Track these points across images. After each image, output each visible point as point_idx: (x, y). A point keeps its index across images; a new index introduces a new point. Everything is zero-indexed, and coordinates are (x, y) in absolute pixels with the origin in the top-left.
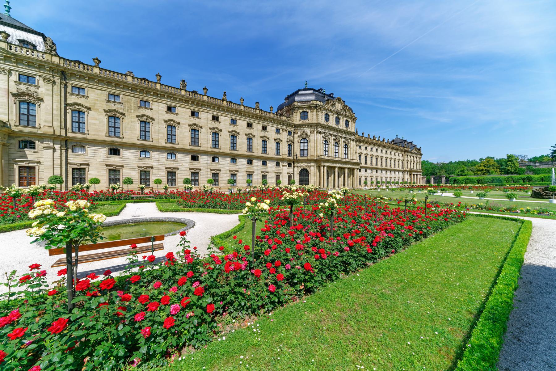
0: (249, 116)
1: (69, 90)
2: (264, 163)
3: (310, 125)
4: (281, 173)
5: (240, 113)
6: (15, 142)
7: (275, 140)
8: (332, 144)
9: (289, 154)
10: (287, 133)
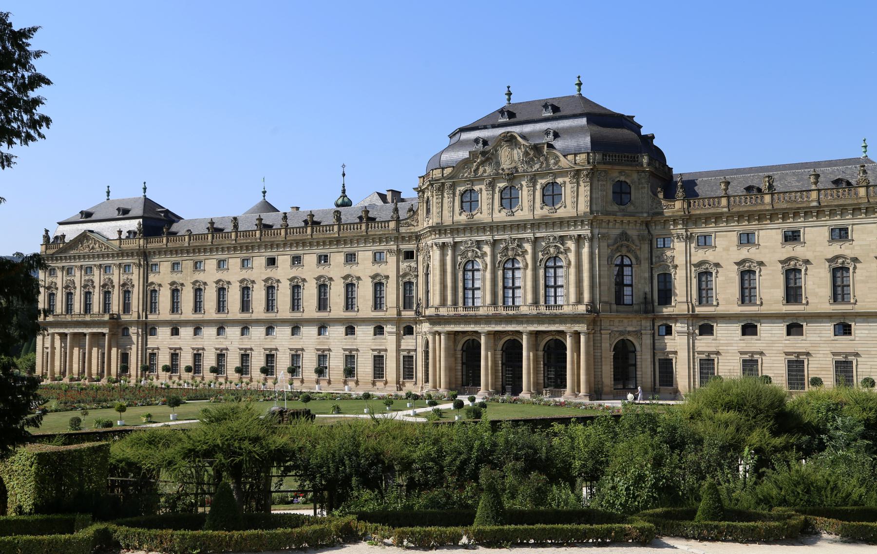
0: (318, 244)
1: (149, 269)
2: (350, 331)
4: (386, 350)
5: (303, 243)
6: (120, 330)
9: (407, 303)
10: (401, 257)
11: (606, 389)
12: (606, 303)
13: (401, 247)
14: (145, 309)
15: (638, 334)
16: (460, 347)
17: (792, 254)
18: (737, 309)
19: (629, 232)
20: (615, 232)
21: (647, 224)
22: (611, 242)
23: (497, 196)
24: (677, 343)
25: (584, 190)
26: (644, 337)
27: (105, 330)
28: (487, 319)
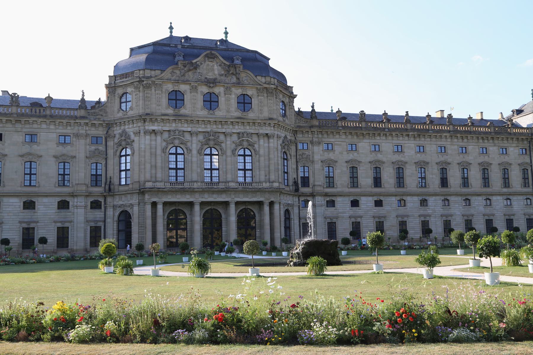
3: (132, 120)
4: (70, 222)
7: (55, 157)
8: (195, 152)
9: (96, 179)
10: (89, 140)
13: (89, 132)
16: (166, 217)
17: (376, 158)
18: (347, 190)
20: (283, 135)
21: (295, 132)
22: (280, 142)
23: (200, 98)
26: (295, 208)
28: (203, 191)
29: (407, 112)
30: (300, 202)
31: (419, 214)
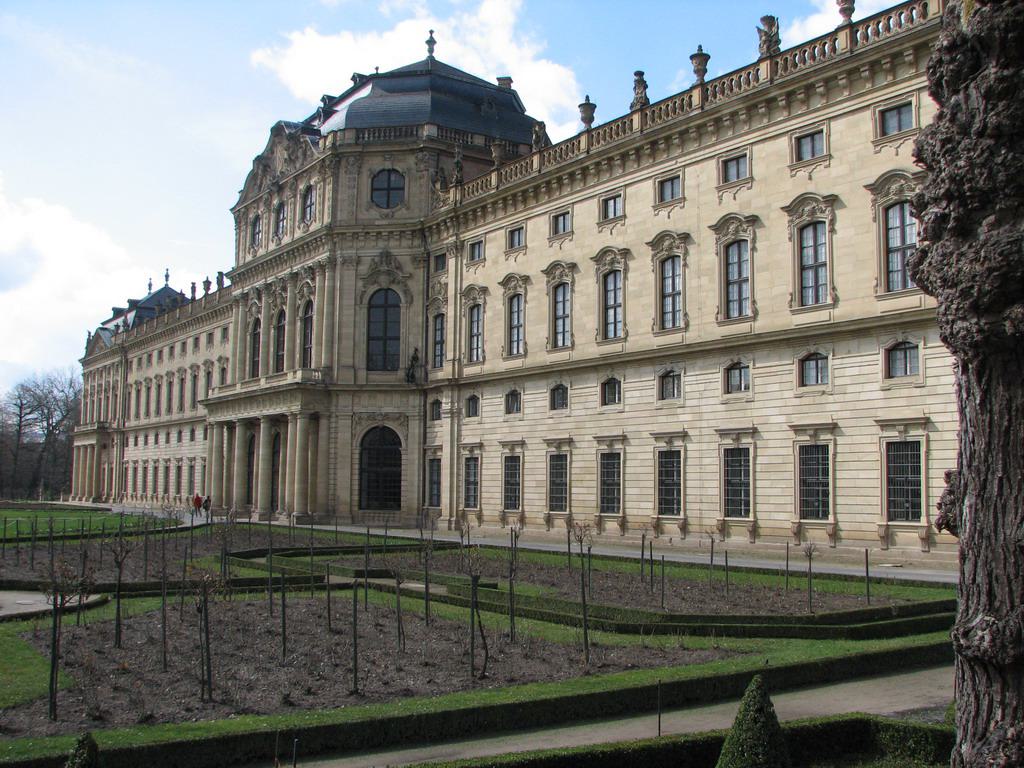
11: (344, 509)
12: (348, 367)
14: (124, 416)
15: (403, 419)
19: (394, 252)
20: (370, 251)
22: (364, 269)
24: (442, 430)
25: (329, 188)
27: (94, 442)
29: (640, 74)
30: (428, 406)
31: (657, 429)
